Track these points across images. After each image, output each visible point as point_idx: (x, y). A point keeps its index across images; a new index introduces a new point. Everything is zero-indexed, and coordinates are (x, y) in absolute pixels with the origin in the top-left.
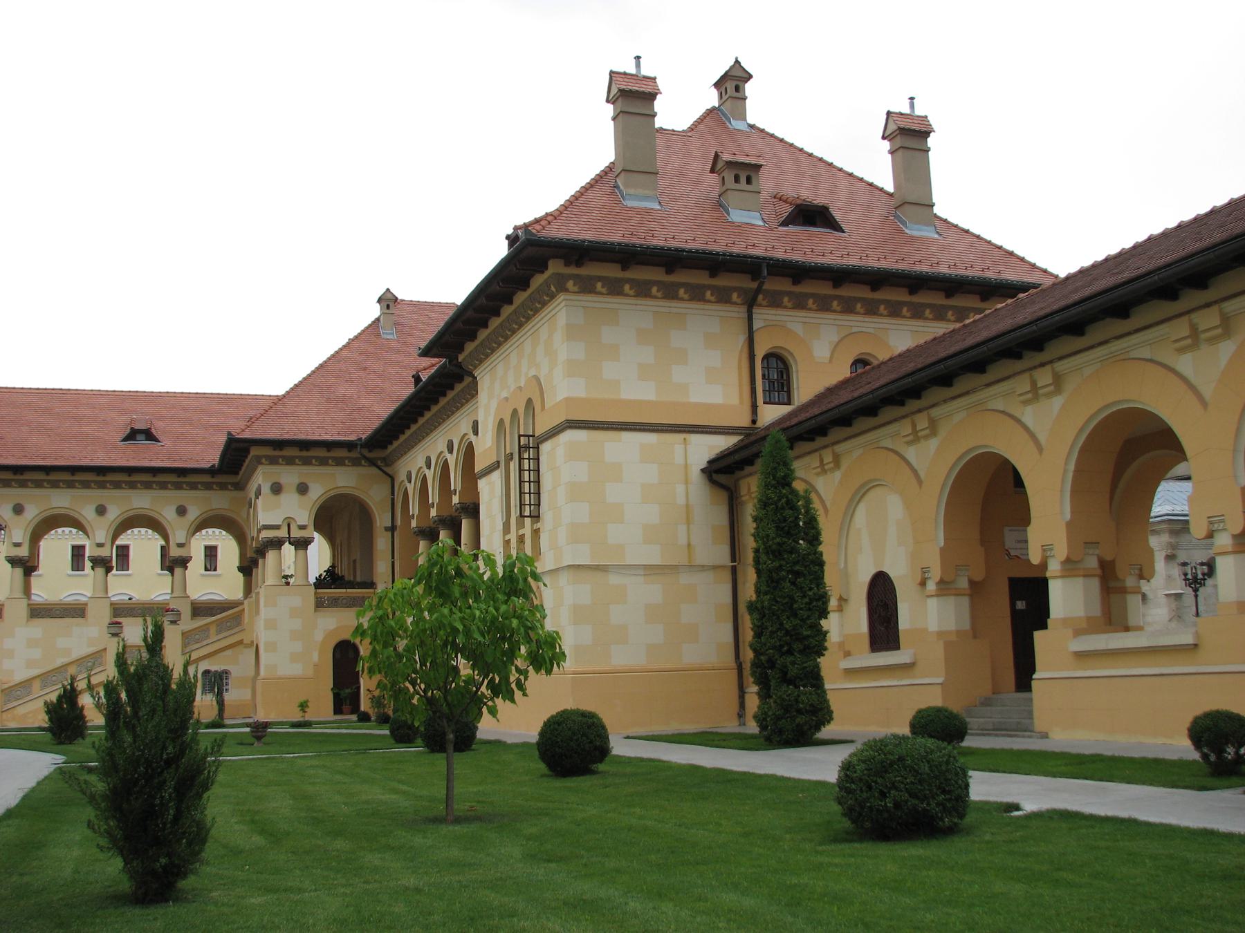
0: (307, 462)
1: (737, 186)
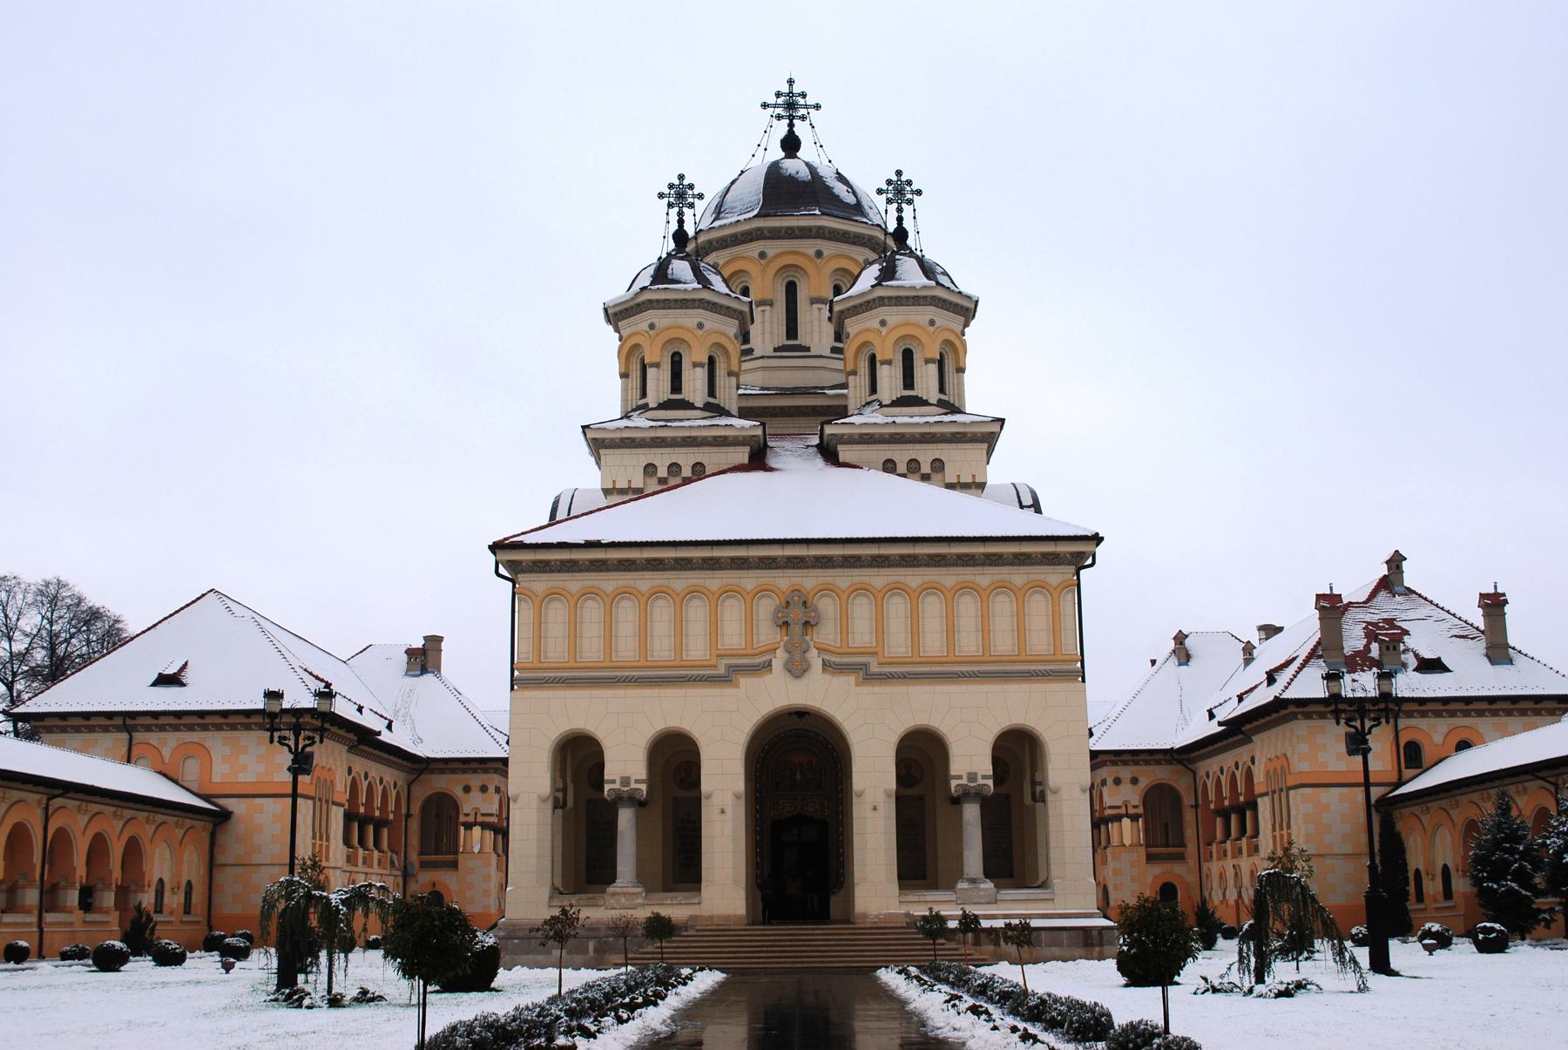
1: (1388, 652)
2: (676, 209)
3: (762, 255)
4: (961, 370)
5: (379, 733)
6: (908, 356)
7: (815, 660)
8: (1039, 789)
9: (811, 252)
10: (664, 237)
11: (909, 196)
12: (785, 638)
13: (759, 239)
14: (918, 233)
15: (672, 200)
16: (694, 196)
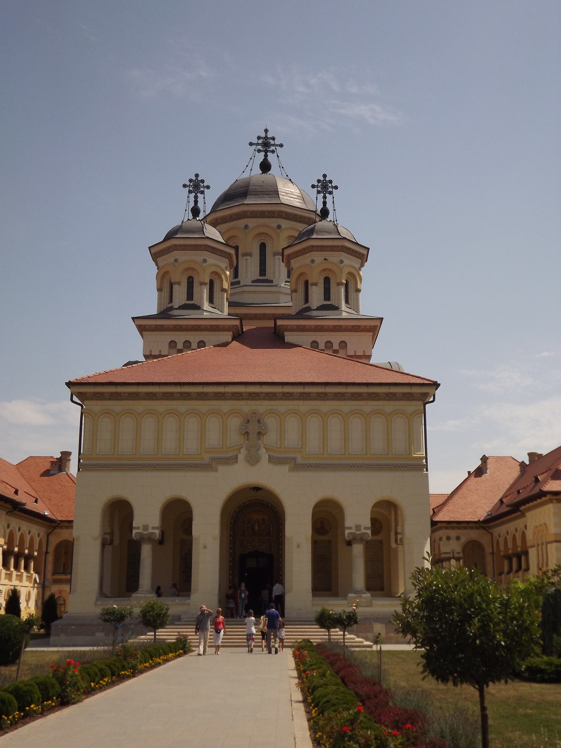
0: (459, 528)
2: (193, 194)
3: (246, 227)
4: (358, 291)
5: (25, 504)
6: (327, 281)
7: (265, 456)
8: (399, 537)
9: (275, 226)
10: (186, 210)
11: (330, 189)
12: (247, 442)
13: (244, 218)
14: (335, 210)
15: (191, 189)
16: (204, 187)
